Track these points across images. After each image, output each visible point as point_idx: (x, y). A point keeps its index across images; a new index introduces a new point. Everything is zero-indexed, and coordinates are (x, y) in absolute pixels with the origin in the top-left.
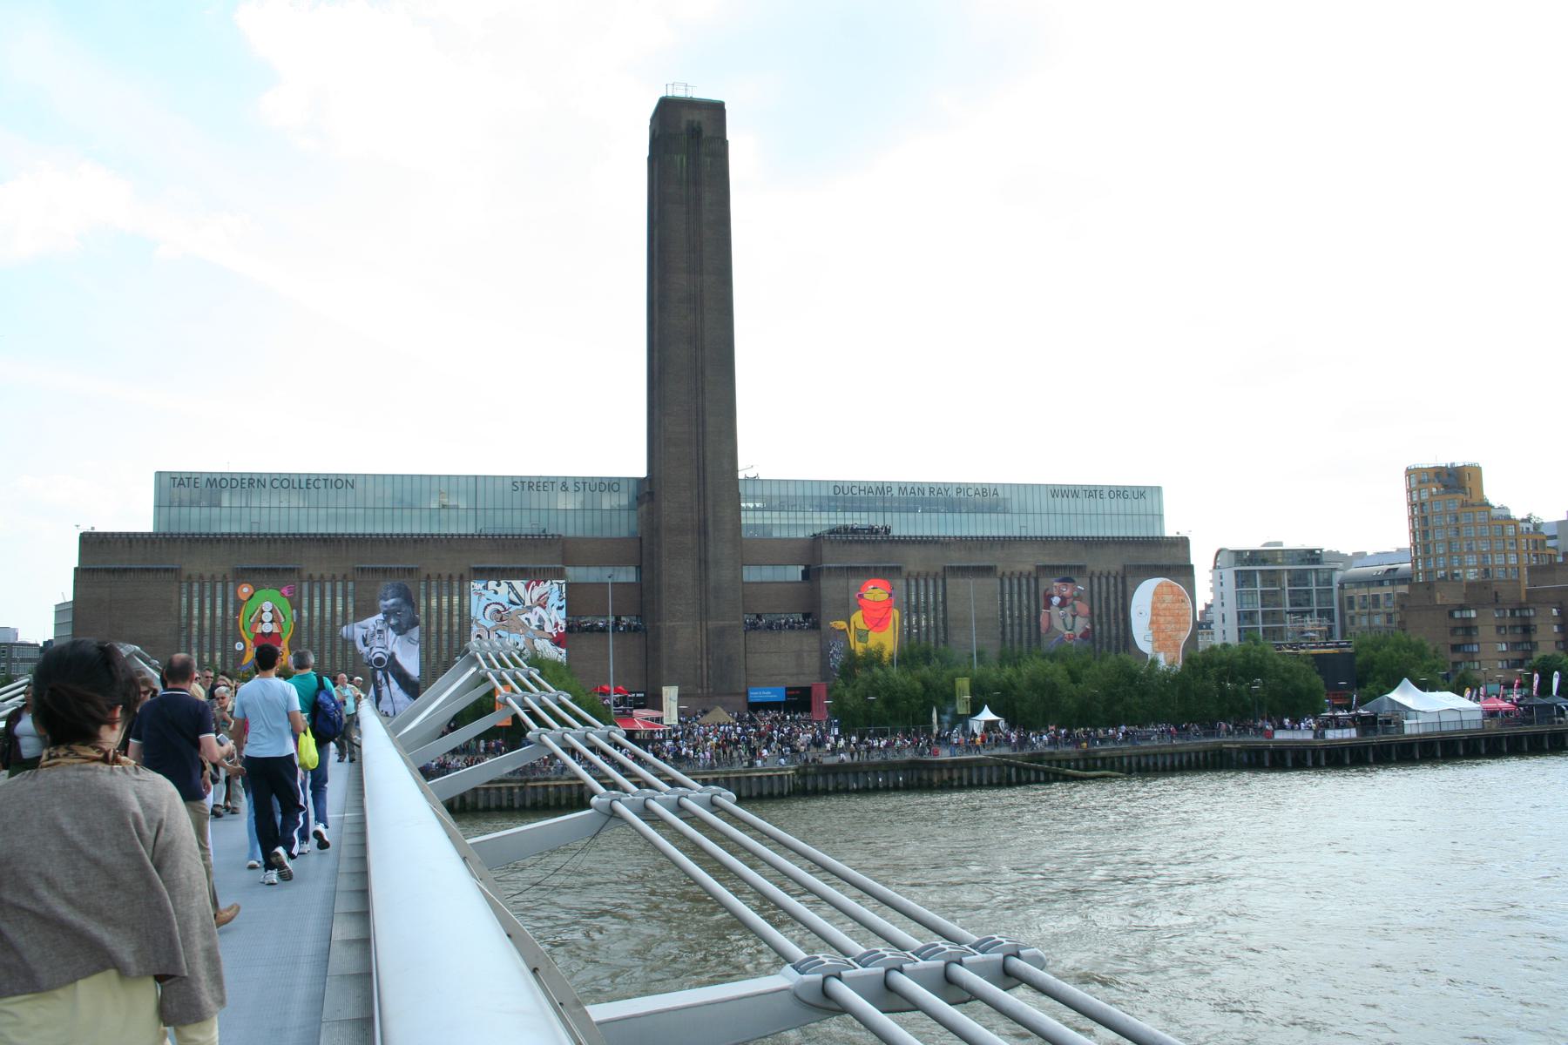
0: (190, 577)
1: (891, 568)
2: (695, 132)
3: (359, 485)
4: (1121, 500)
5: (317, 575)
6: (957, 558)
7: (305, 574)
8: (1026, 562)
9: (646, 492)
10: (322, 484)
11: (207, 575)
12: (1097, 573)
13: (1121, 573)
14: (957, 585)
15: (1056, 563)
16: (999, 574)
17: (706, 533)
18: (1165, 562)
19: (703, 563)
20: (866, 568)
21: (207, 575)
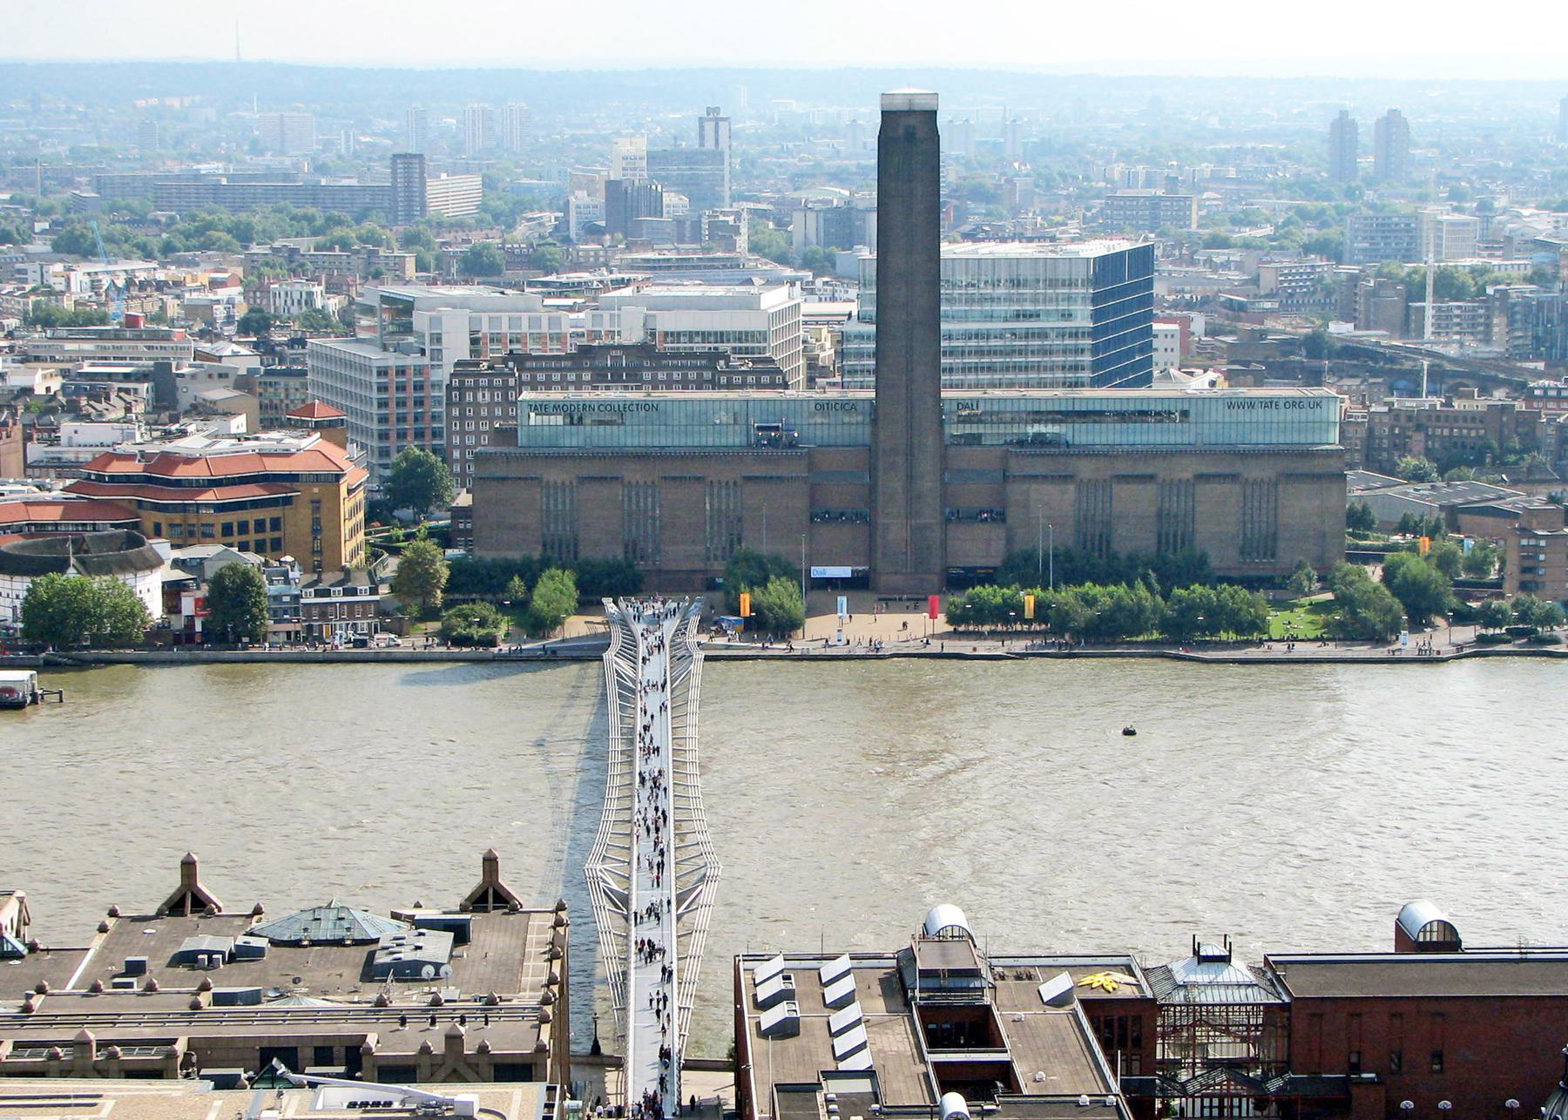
0: (548, 483)
1: (1065, 477)
2: (910, 136)
3: (661, 406)
4: (1296, 411)
5: (634, 482)
6: (1124, 468)
7: (626, 482)
8: (1186, 470)
9: (875, 412)
10: (634, 407)
11: (559, 482)
12: (1251, 480)
13: (1273, 479)
14: (1123, 492)
15: (1213, 470)
16: (1160, 481)
17: (912, 454)
18: (1317, 471)
19: (910, 478)
20: (1045, 477)
21: (559, 482)
